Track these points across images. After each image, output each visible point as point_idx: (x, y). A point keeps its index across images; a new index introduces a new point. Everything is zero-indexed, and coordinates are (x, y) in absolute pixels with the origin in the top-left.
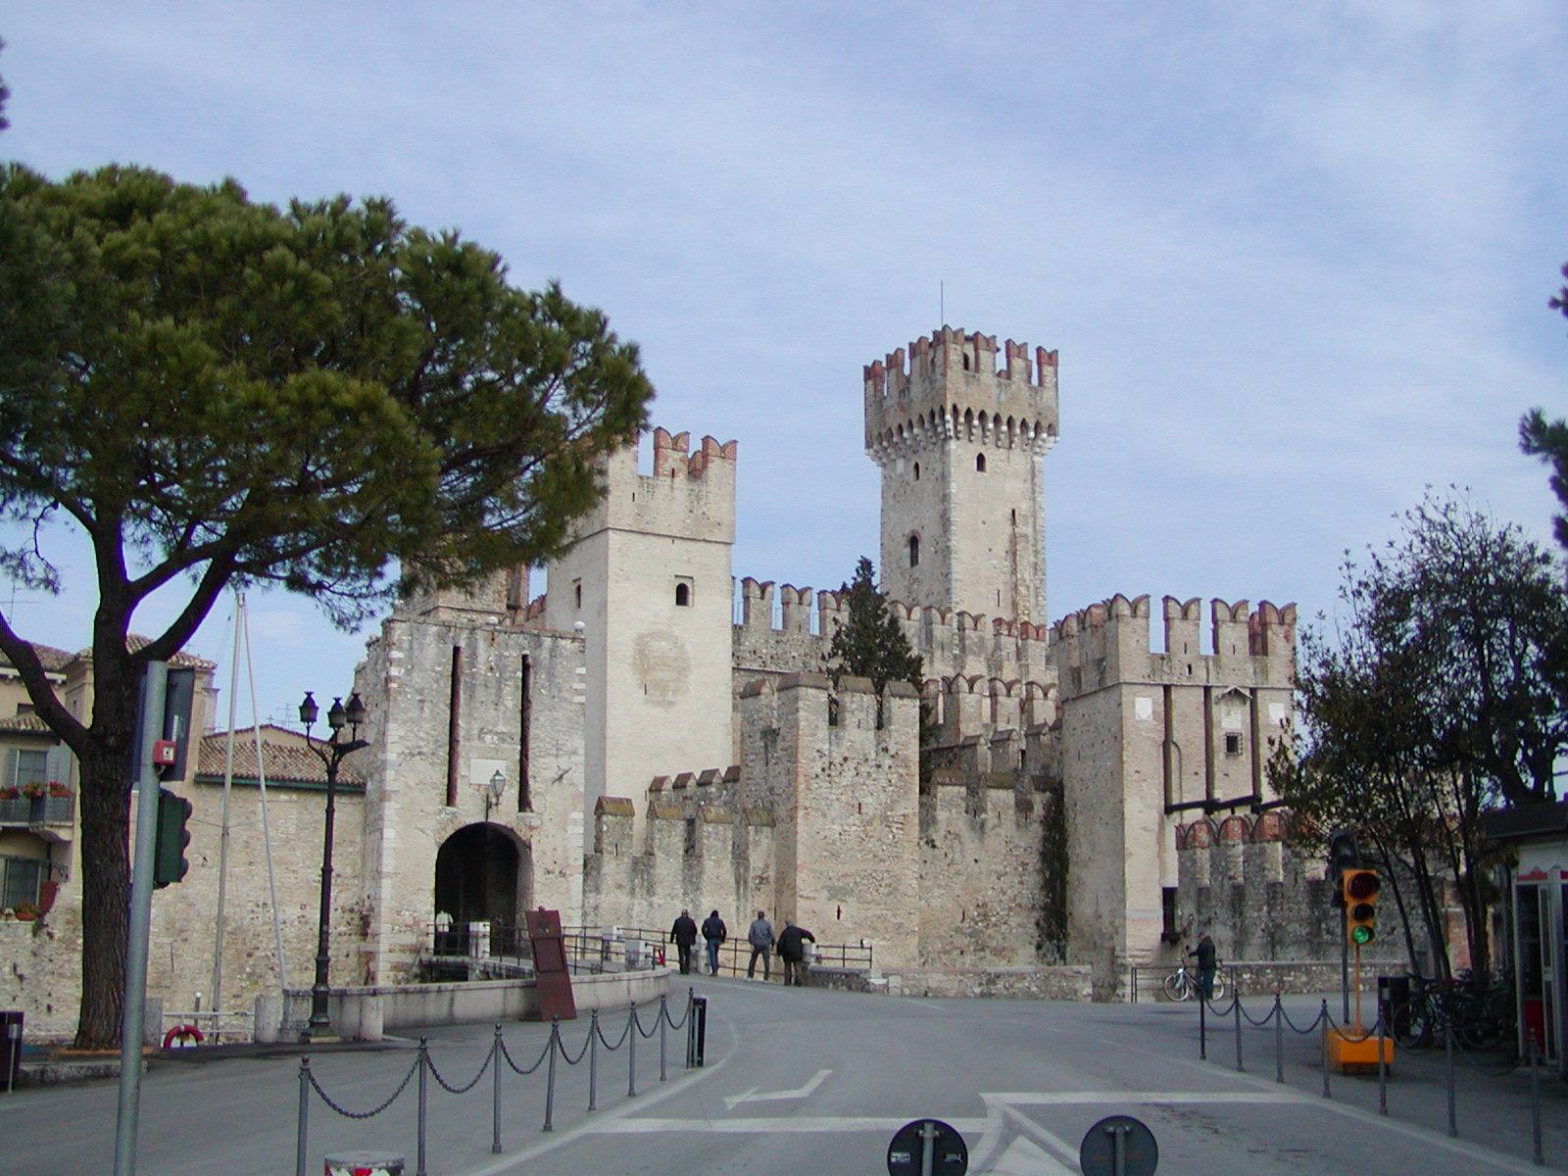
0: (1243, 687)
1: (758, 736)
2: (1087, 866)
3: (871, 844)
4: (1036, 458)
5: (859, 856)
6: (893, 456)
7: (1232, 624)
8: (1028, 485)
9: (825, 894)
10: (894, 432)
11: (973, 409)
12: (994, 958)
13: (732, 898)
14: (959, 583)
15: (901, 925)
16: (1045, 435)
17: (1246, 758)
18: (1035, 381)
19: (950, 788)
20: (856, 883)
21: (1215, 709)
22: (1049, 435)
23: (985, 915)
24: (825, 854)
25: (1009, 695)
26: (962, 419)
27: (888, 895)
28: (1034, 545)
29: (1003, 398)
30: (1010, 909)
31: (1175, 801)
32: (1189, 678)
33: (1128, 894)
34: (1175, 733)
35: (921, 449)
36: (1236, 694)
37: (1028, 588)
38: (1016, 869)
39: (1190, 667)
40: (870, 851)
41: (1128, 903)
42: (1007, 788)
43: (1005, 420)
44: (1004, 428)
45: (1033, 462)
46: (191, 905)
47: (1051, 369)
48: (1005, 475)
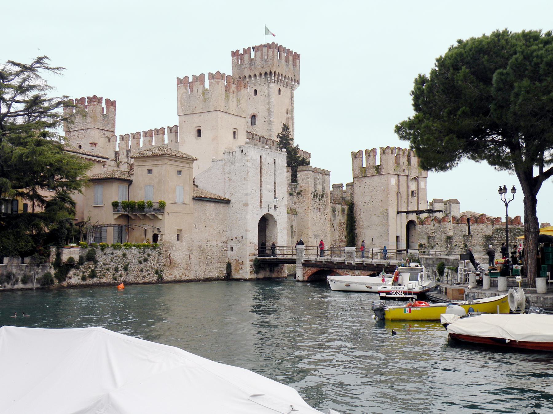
3: (322, 221)
4: (293, 91)
9: (313, 237)
10: (247, 77)
17: (416, 198)
21: (409, 183)
36: (415, 179)
39: (404, 170)
46: (193, 241)
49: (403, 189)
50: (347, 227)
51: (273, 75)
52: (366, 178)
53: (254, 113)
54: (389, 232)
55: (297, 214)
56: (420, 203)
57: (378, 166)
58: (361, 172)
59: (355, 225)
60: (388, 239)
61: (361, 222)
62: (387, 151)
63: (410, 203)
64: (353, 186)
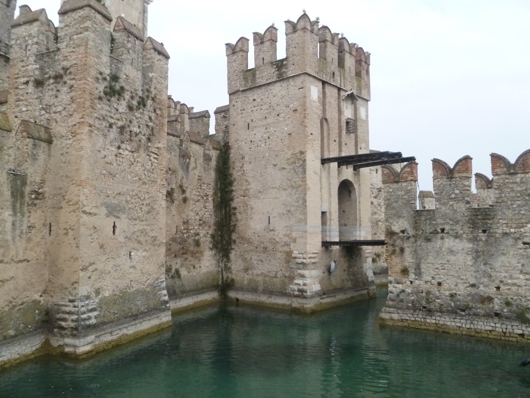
1: (32, 59)
2: (257, 197)
3: (138, 168)
4: (145, 4)
5: (129, 177)
9: (104, 211)
12: (192, 259)
13: (7, 214)
15: (155, 239)
19: (171, 137)
20: (127, 202)
21: (342, 104)
23: (187, 229)
24: (104, 172)
27: (149, 212)
30: (200, 225)
31: (326, 157)
32: (334, 81)
33: (309, 215)
36: (352, 97)
38: (203, 198)
39: (334, 74)
40: (137, 175)
41: (308, 221)
42: (200, 144)
45: (144, 6)
48: (132, 7)
49: (332, 114)
50: (215, 194)
52: (255, 90)
54: (308, 203)
55: (49, 142)
56: (359, 146)
57: (282, 61)
58: (245, 79)
59: (232, 191)
60: (306, 219)
61: (245, 183)
63: (343, 144)
64: (228, 110)
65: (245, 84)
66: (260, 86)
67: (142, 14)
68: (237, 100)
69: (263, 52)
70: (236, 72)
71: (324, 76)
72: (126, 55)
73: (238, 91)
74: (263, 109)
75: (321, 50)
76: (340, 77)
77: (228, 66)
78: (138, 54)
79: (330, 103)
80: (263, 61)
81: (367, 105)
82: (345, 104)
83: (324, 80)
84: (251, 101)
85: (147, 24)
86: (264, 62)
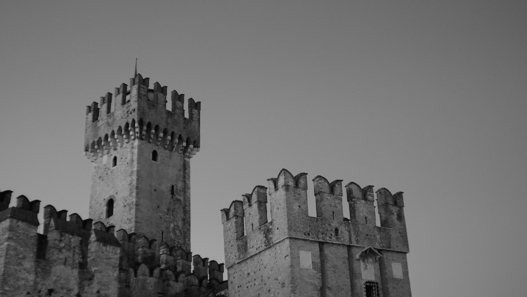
0: (375, 249)
6: (100, 155)
7: (363, 201)
8: (182, 173)
10: (103, 139)
11: (152, 123)
14: (139, 224)
16: (191, 146)
18: (187, 116)
21: (356, 264)
22: (194, 147)
25: (176, 280)
26: (145, 128)
28: (184, 208)
29: (170, 121)
32: (337, 239)
34: (329, 280)
35: (118, 148)
37: (180, 231)
39: (337, 230)
43: (170, 133)
44: (169, 138)
45: (185, 161)
47: (196, 111)
51: (136, 125)
52: (248, 261)
53: (111, 196)
62: (281, 182)
65: (239, 256)
66: (252, 257)
67: (182, 171)
68: (234, 275)
69: (253, 216)
70: (232, 242)
71: (320, 236)
72: (57, 256)
73: (234, 264)
74: (257, 284)
75: (318, 204)
76: (349, 232)
77: (224, 236)
78: (74, 251)
79: (335, 266)
80: (253, 227)
81: (405, 258)
82: (362, 263)
83: (321, 240)
84: (246, 276)
85: (189, 181)
86: (253, 228)
